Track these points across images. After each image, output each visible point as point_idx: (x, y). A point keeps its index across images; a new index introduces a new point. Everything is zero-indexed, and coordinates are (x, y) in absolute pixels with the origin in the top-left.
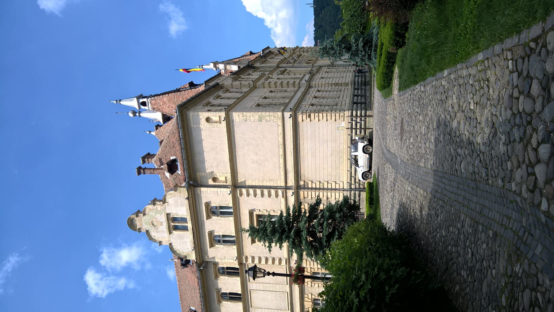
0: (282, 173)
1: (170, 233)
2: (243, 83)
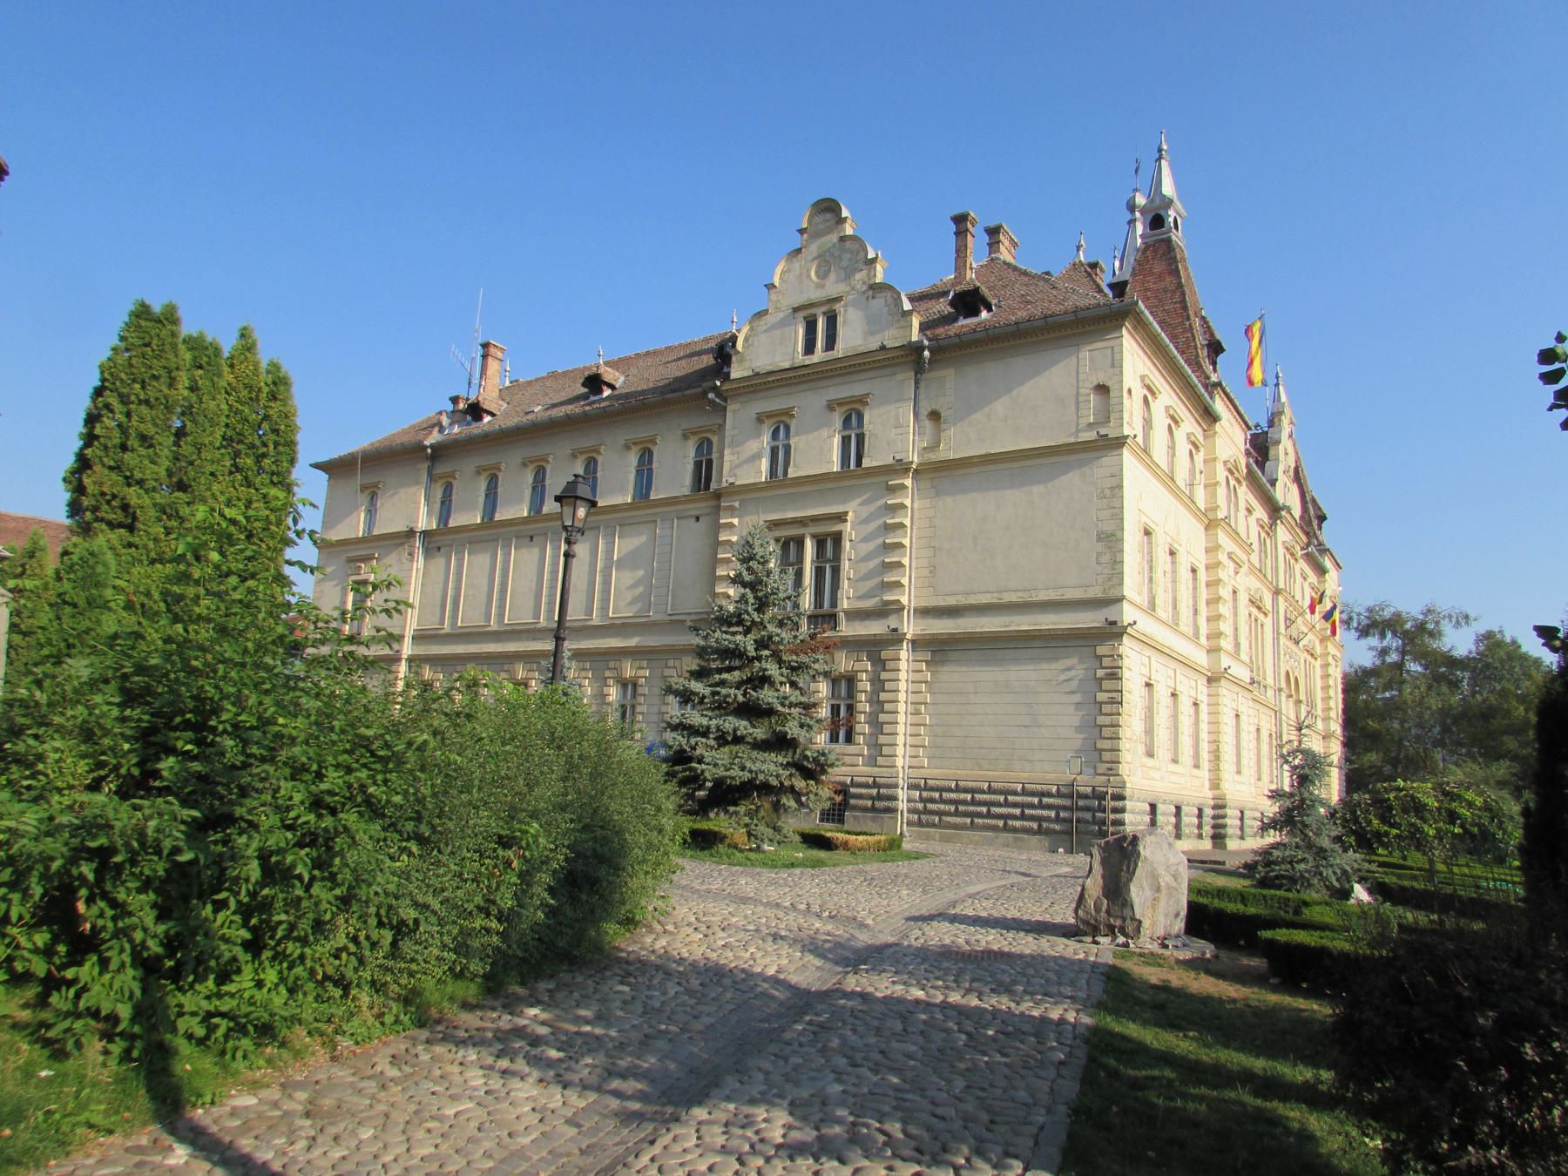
0: (951, 601)
1: (796, 310)
2: (1221, 491)
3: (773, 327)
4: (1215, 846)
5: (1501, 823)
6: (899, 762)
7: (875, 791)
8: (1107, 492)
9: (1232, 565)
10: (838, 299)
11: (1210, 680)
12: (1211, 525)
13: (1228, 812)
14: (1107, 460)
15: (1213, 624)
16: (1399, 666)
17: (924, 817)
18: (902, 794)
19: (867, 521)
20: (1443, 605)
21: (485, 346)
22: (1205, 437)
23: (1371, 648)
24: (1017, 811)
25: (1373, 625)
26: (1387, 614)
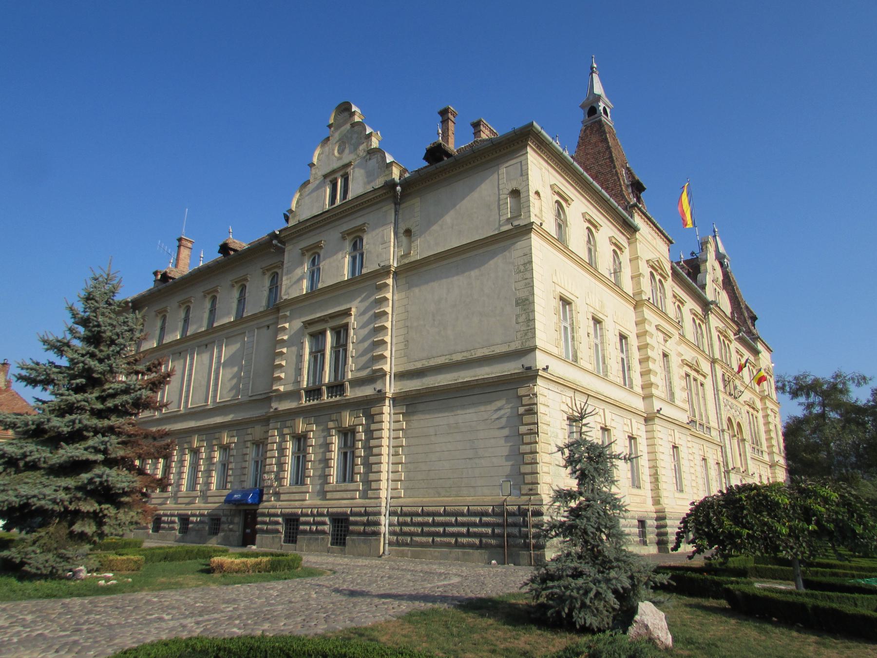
0: (419, 365)
3: (313, 191)
4: (660, 550)
5: (861, 517)
6: (383, 494)
7: (365, 519)
8: (522, 268)
9: (661, 335)
10: (348, 165)
11: (646, 420)
12: (638, 305)
13: (668, 522)
14: (520, 244)
15: (646, 378)
16: (823, 415)
17: (402, 538)
18: (384, 520)
19: (364, 313)
20: (848, 371)
21: (180, 240)
22: (629, 244)
23: (800, 404)
24: (464, 530)
25: (800, 388)
26: (809, 380)
